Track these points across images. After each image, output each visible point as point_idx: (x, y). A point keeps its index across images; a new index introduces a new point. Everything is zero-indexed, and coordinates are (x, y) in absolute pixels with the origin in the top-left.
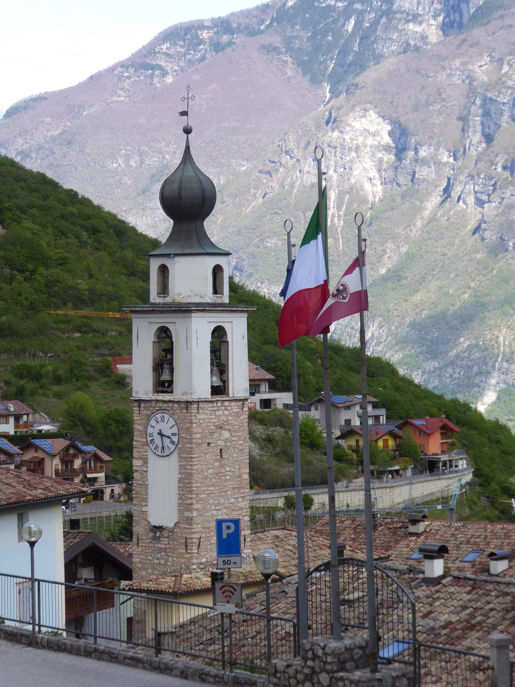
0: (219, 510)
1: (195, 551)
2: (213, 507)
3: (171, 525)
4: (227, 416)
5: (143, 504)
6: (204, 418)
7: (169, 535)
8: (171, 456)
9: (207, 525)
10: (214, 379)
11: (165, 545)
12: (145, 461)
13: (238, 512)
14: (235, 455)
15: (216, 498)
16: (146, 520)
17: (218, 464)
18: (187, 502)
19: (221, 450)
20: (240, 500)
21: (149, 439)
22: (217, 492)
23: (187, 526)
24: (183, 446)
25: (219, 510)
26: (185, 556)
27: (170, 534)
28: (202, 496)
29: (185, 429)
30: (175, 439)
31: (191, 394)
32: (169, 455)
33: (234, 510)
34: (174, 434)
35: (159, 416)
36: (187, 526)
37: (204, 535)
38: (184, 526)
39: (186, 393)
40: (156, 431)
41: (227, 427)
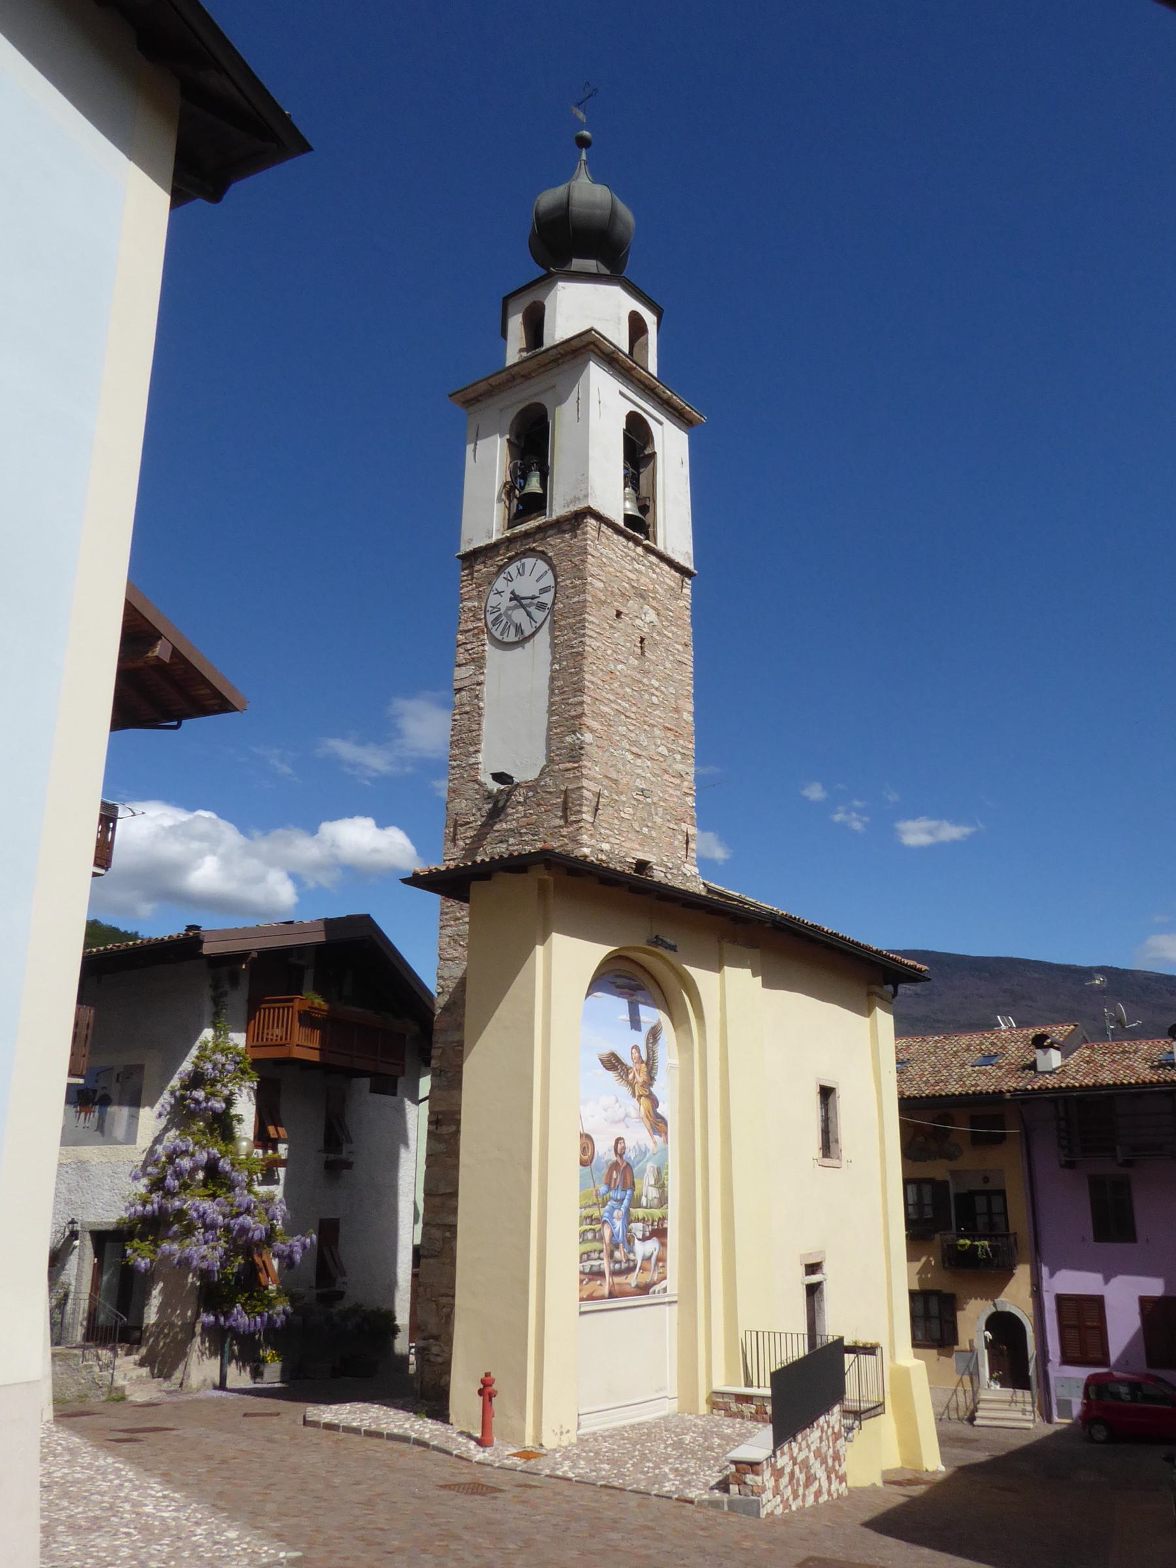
0: (638, 756)
1: (587, 817)
2: (625, 744)
3: (532, 775)
4: (651, 579)
5: (472, 749)
6: (608, 556)
7: (526, 798)
8: (537, 637)
9: (614, 775)
10: (628, 505)
11: (517, 820)
12: (478, 661)
13: (672, 780)
14: (668, 665)
15: (632, 728)
16: (476, 781)
17: (636, 662)
18: (573, 713)
19: (642, 640)
20: (678, 757)
21: (490, 618)
22: (632, 715)
23: (569, 765)
24: (565, 621)
25: (638, 756)
26: (564, 832)
27: (530, 794)
28: (605, 709)
29: (570, 576)
30: (547, 598)
31: (586, 496)
32: (533, 634)
33: (666, 771)
34: (544, 590)
35: (512, 569)
36: (569, 765)
37: (606, 793)
38: (562, 766)
39: (577, 499)
40: (504, 602)
41: (654, 603)
